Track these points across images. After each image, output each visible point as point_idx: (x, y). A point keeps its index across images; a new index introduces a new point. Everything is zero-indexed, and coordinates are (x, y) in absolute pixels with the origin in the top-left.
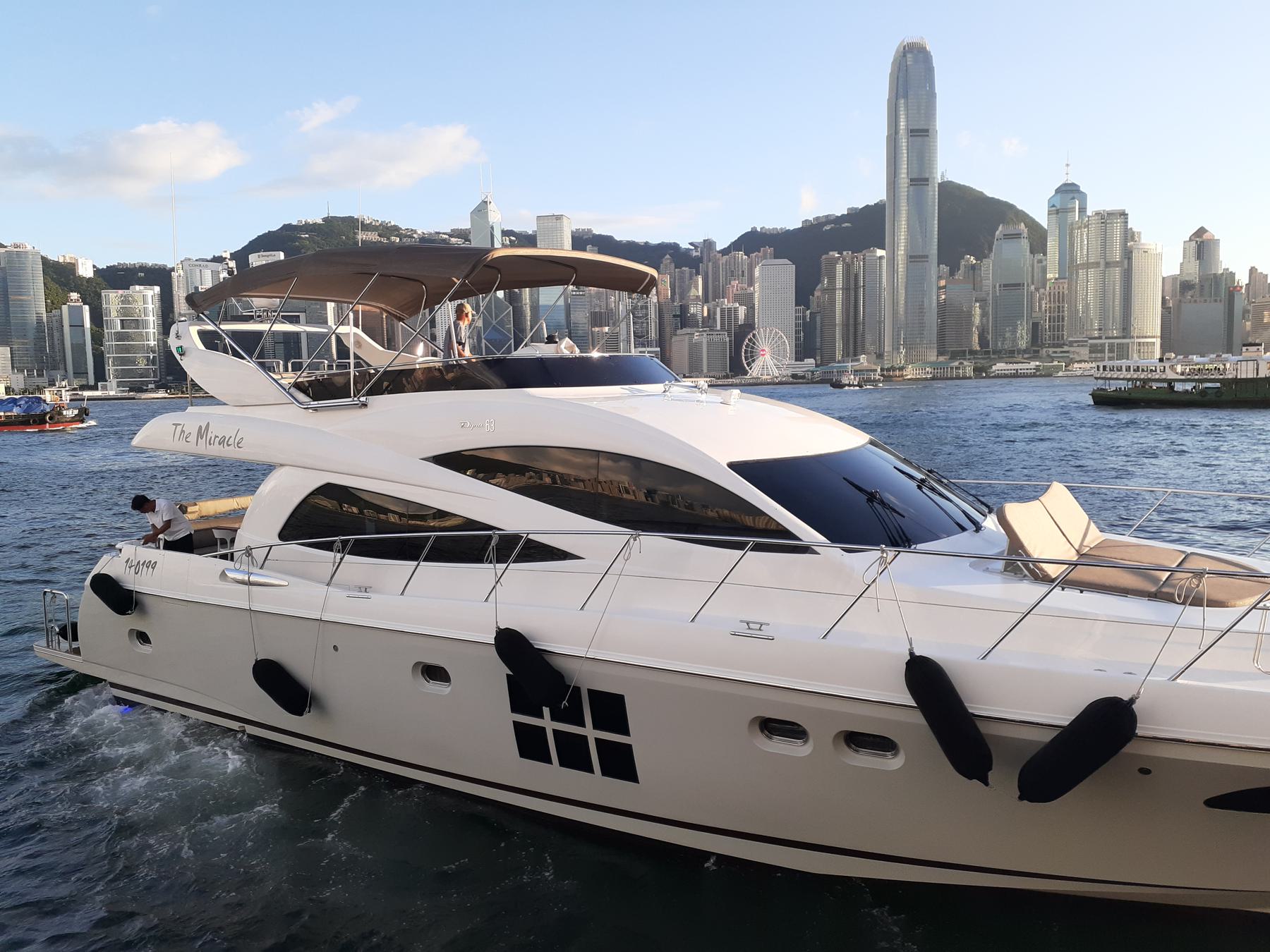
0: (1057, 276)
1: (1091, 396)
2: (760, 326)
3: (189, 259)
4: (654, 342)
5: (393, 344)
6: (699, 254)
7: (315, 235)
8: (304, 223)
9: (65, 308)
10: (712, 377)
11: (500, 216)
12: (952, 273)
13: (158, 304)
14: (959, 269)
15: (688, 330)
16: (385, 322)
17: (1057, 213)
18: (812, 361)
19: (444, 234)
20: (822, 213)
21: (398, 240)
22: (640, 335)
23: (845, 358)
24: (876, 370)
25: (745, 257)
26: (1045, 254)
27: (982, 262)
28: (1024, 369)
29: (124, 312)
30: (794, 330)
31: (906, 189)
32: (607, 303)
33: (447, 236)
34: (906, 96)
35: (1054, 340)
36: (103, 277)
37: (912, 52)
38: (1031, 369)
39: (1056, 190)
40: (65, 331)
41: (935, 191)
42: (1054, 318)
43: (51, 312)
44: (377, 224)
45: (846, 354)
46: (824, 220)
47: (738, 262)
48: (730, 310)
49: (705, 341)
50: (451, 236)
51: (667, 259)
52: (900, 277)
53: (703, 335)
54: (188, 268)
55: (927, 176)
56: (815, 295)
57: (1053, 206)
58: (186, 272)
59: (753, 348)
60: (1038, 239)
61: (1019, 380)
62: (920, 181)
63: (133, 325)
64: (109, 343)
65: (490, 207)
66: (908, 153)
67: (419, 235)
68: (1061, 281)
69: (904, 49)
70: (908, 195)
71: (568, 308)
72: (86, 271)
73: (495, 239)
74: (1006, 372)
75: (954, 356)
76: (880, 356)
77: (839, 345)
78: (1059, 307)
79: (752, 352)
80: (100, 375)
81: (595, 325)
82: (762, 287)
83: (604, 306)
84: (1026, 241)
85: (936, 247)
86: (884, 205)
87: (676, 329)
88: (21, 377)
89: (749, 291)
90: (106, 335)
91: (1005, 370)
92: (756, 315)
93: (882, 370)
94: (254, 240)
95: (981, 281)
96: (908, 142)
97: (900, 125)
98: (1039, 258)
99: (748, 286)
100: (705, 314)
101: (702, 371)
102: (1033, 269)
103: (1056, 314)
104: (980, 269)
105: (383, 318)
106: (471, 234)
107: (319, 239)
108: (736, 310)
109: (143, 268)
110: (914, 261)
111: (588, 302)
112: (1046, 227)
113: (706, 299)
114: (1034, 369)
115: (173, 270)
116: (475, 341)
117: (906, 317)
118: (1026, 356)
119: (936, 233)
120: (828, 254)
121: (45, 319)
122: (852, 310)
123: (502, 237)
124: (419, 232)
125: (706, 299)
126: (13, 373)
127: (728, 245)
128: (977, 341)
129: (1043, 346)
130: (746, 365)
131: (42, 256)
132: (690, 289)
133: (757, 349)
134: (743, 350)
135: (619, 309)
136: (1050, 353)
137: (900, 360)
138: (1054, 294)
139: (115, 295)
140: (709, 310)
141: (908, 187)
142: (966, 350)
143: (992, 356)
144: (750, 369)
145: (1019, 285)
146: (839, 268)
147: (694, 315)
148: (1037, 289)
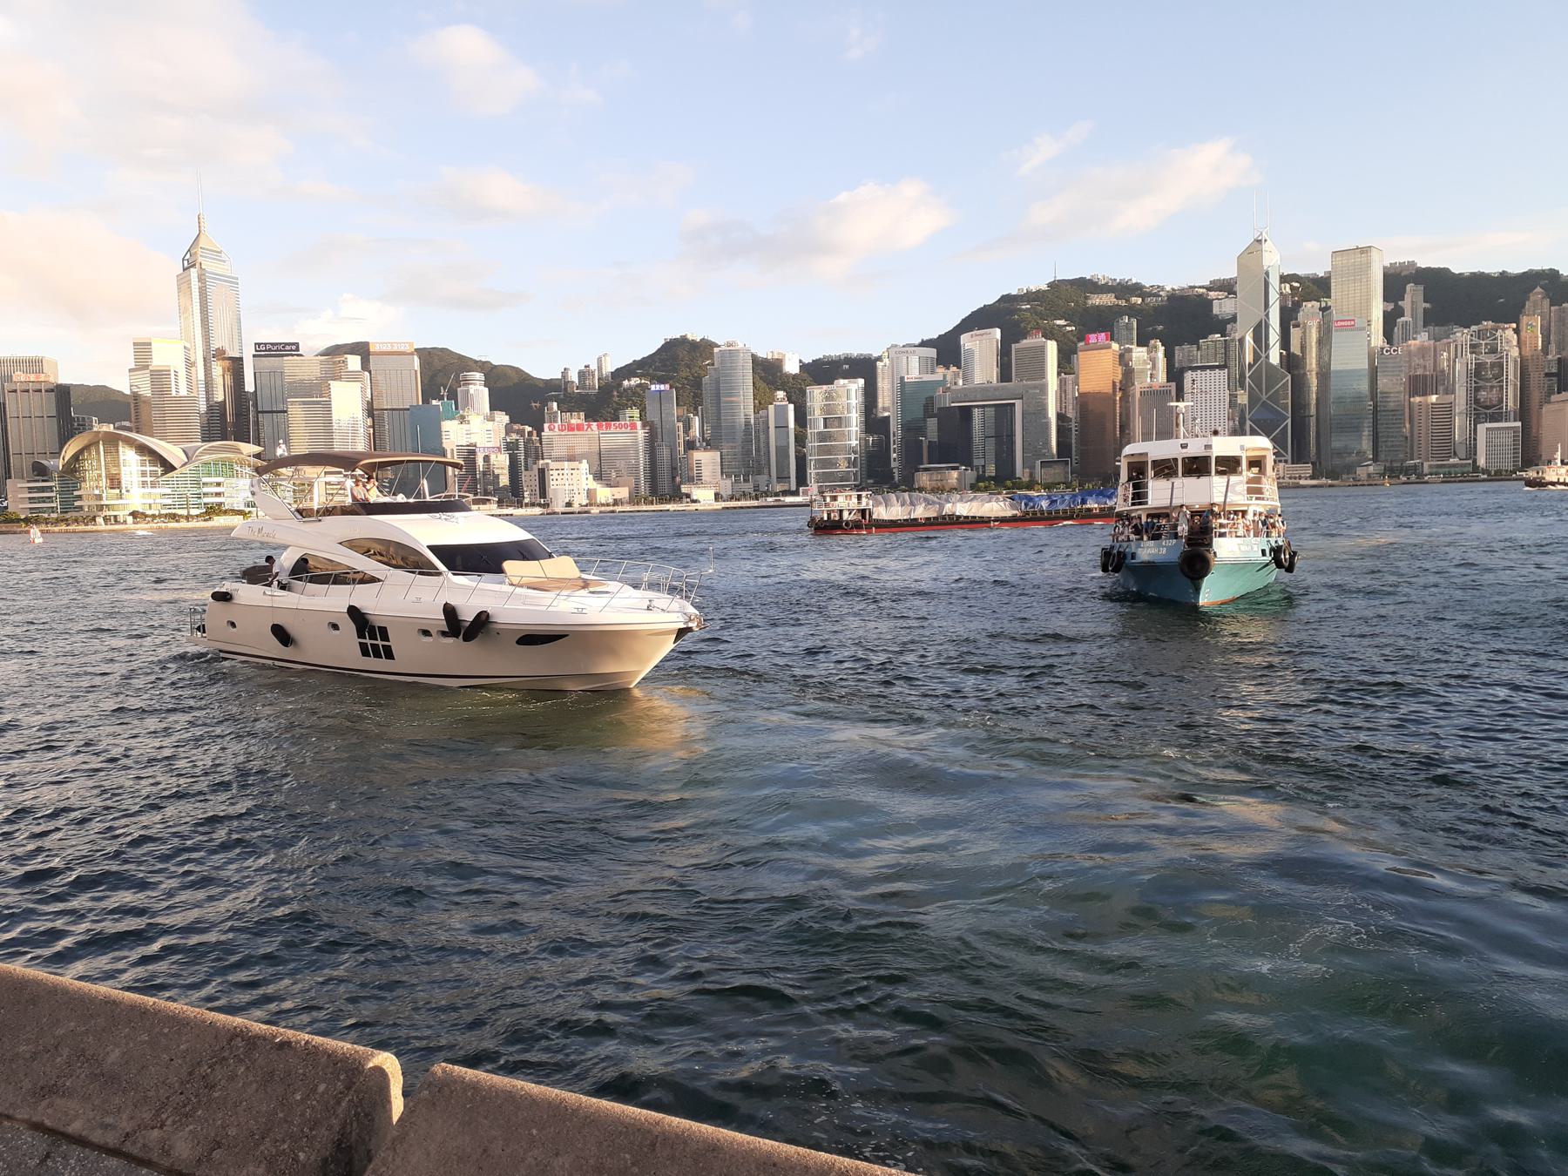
3: (896, 346)
4: (1512, 414)
9: (771, 408)
11: (1278, 257)
13: (861, 399)
29: (827, 409)
32: (1435, 361)
33: (1204, 290)
50: (1209, 289)
51: (1539, 293)
58: (892, 362)
63: (836, 423)
64: (812, 444)
65: (1265, 246)
72: (792, 367)
80: (802, 480)
83: (1430, 364)
87: (1550, 393)
88: (728, 482)
105: (1115, 400)
109: (848, 360)
111: (1405, 362)
115: (879, 359)
116: (1237, 423)
121: (752, 421)
131: (753, 355)
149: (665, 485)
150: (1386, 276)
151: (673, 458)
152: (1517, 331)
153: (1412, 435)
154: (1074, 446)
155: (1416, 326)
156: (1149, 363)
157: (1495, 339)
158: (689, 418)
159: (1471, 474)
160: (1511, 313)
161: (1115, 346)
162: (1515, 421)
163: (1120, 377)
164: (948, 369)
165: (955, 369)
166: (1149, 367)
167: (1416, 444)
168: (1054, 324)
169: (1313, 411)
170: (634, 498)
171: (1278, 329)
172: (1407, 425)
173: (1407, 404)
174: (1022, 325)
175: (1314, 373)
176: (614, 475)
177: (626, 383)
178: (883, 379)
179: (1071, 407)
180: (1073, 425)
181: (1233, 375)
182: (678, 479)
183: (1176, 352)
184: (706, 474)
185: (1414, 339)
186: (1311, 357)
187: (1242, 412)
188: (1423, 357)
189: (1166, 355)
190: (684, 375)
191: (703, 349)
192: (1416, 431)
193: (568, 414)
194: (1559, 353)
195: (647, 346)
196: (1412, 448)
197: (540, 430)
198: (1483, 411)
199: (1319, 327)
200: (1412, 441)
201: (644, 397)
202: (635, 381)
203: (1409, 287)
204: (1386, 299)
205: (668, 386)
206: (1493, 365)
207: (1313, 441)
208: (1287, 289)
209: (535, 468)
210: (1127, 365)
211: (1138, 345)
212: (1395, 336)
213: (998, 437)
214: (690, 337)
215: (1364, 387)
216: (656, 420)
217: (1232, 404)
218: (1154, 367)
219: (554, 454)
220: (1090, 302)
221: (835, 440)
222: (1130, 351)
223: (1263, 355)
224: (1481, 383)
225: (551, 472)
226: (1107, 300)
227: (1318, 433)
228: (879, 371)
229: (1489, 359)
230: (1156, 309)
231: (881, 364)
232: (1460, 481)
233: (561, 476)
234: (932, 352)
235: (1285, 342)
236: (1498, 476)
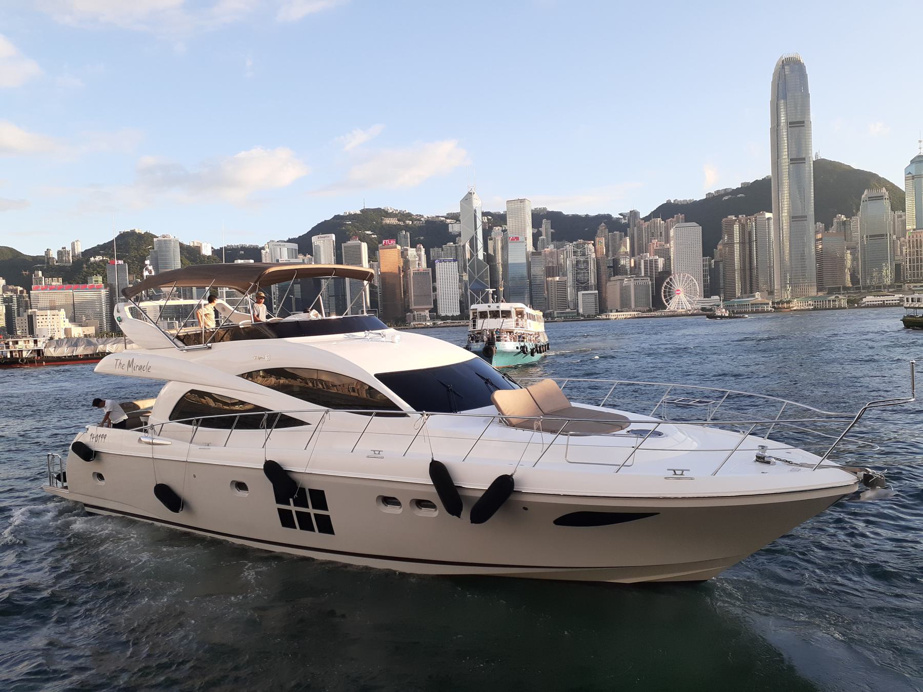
0: (915, 227)
1: (902, 322)
2: (676, 272)
4: (594, 286)
5: (407, 294)
6: (627, 221)
8: (348, 214)
10: (638, 311)
11: (480, 202)
12: (827, 228)
14: (832, 225)
15: (620, 277)
16: (402, 280)
17: (913, 179)
18: (717, 297)
19: (442, 217)
20: (721, 187)
21: (411, 223)
22: (583, 282)
23: (744, 295)
24: (768, 304)
25: (662, 222)
26: (904, 211)
27: (851, 219)
28: (889, 301)
30: (702, 275)
31: (787, 167)
32: (557, 260)
33: (444, 219)
34: (785, 98)
35: (914, 277)
36: (217, 255)
37: (788, 65)
38: (895, 300)
39: (911, 161)
40: (193, 291)
41: (810, 167)
42: (914, 260)
44: (397, 213)
45: (744, 291)
46: (723, 192)
47: (657, 226)
48: (651, 261)
49: (632, 284)
50: (446, 218)
51: (603, 226)
52: (784, 233)
53: (630, 280)
55: (804, 156)
56: (718, 249)
57: (910, 173)
58: (271, 250)
59: (670, 289)
60: (898, 200)
61: (886, 309)
62: (798, 161)
65: (474, 196)
66: (788, 140)
68: (918, 231)
69: (783, 62)
70: (789, 171)
71: (529, 265)
73: (477, 218)
74: (875, 303)
75: (831, 291)
76: (771, 293)
77: (738, 285)
78: (917, 251)
79: (669, 292)
81: (548, 276)
82: (676, 244)
83: (555, 261)
84: (888, 201)
85: (813, 209)
86: (770, 179)
87: (610, 276)
89: (666, 247)
90: (219, 293)
91: (873, 301)
92: (672, 264)
93: (773, 303)
95: (851, 233)
96: (787, 132)
97: (781, 120)
98: (899, 214)
99: (665, 243)
100: (633, 265)
101: (631, 306)
102: (894, 223)
103: (916, 257)
104: (850, 225)
105: (400, 277)
107: (358, 224)
108: (656, 261)
109: (243, 248)
110: (796, 221)
111: (544, 259)
112: (904, 190)
113: (633, 254)
114: (898, 300)
115: (263, 248)
117: (791, 263)
118: (891, 290)
119: (813, 198)
120: (727, 217)
122: (747, 257)
125: (633, 254)
126: (161, 321)
127: (649, 213)
128: (849, 280)
129: (905, 282)
130: (665, 302)
131: (180, 243)
132: (620, 247)
133: (673, 290)
134: (663, 291)
135: (566, 265)
136: (911, 287)
137: (787, 296)
138: (913, 241)
140: (635, 262)
141: (788, 165)
142: (840, 287)
143: (863, 291)
144: (669, 304)
145: (882, 235)
146: (736, 227)
147: (624, 266)
148: (898, 238)
150: (533, 214)
152: (594, 245)
153: (548, 297)
154: (379, 302)
155: (548, 241)
156: (417, 257)
157: (584, 249)
159: (576, 317)
160: (591, 236)
161: (399, 247)
162: (595, 290)
163: (402, 264)
164: (305, 256)
165: (309, 256)
167: (550, 301)
168: (365, 233)
172: (546, 292)
173: (545, 281)
174: (347, 233)
176: (84, 318)
177: (92, 259)
179: (377, 280)
180: (378, 290)
185: (548, 248)
188: (552, 257)
190: (133, 254)
191: (147, 238)
192: (550, 295)
193: (50, 279)
194: (613, 256)
195: (108, 235)
196: (548, 303)
197: (29, 289)
198: (581, 285)
199: (502, 241)
200: (548, 300)
203: (544, 221)
204: (533, 227)
206: (584, 262)
209: (25, 315)
210: (405, 258)
211: (411, 247)
212: (538, 246)
213: (336, 296)
214: (137, 231)
215: (525, 273)
217: (461, 280)
219: (39, 305)
221: (236, 297)
222: (407, 250)
223: (475, 255)
224: (579, 271)
225: (37, 318)
226: (393, 221)
228: (263, 256)
229: (582, 259)
230: (420, 227)
232: (571, 321)
233: (45, 320)
234: (295, 246)
235: (486, 248)
236: (589, 318)
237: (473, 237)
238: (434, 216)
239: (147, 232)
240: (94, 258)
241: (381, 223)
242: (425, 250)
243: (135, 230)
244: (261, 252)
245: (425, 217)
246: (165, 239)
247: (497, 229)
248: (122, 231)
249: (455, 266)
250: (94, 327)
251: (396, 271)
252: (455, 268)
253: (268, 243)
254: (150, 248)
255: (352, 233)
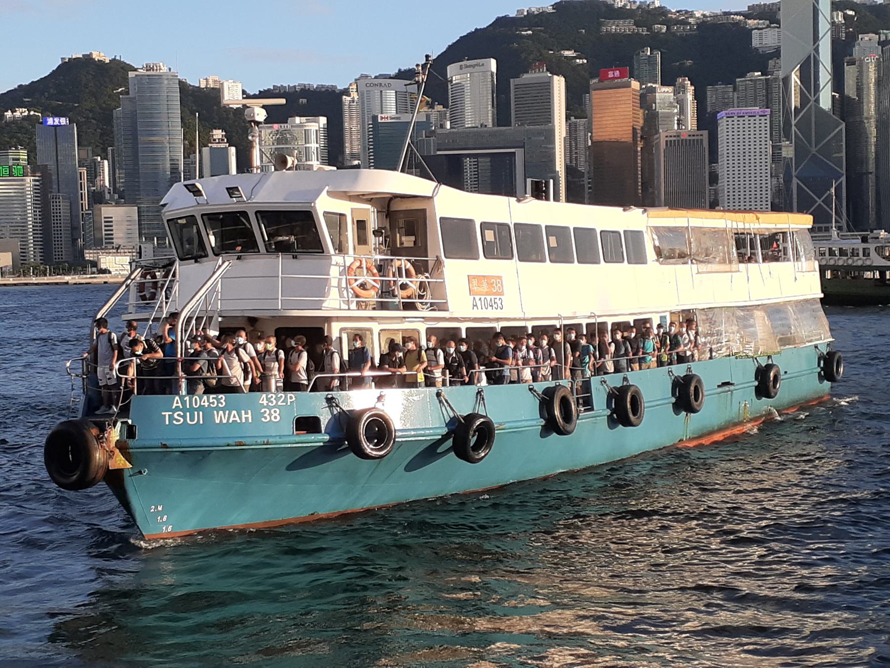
5: (651, 190)
7: (541, 31)
21: (664, 29)
43: (189, 158)
44: (634, 7)
50: (747, 16)
54: (365, 89)
67: (698, 18)
73: (821, 16)
94: (454, 44)
105: (637, 152)
106: (781, 12)
109: (305, 92)
115: (346, 92)
116: (782, 180)
123: (832, 11)
124: (698, 14)
139: (270, 131)
149: (63, 251)
151: (73, 216)
158: (95, 162)
161: (635, 85)
163: (641, 122)
165: (440, 108)
166: (676, 111)
168: (562, 56)
169: (872, 167)
170: (20, 267)
171: (829, 66)
174: (523, 56)
175: (873, 121)
177: (9, 114)
178: (351, 118)
180: (586, 180)
181: (776, 123)
182: (80, 242)
183: (709, 93)
184: (119, 237)
186: (869, 102)
187: (788, 167)
189: (696, 96)
201: (33, 134)
202: (20, 113)
205: (63, 121)
207: (871, 203)
208: (840, 18)
211: (662, 84)
214: (96, 56)
216: (51, 165)
217: (776, 157)
218: (682, 111)
220: (604, 29)
222: (653, 90)
223: (812, 99)
226: (624, 27)
227: (878, 193)
228: (346, 108)
230: (684, 39)
231: (349, 99)
235: (838, 82)
237: (810, 56)
238: (719, 12)
239: (114, 59)
240: (12, 112)
241: (598, 30)
242: (695, 90)
243: (91, 54)
244: (341, 98)
245: (698, 14)
246: (151, 73)
247: (867, 38)
248: (68, 56)
249: (763, 125)
250: (10, 254)
251: (627, 137)
252: (763, 129)
253: (356, 80)
254: (121, 93)
255: (531, 57)
